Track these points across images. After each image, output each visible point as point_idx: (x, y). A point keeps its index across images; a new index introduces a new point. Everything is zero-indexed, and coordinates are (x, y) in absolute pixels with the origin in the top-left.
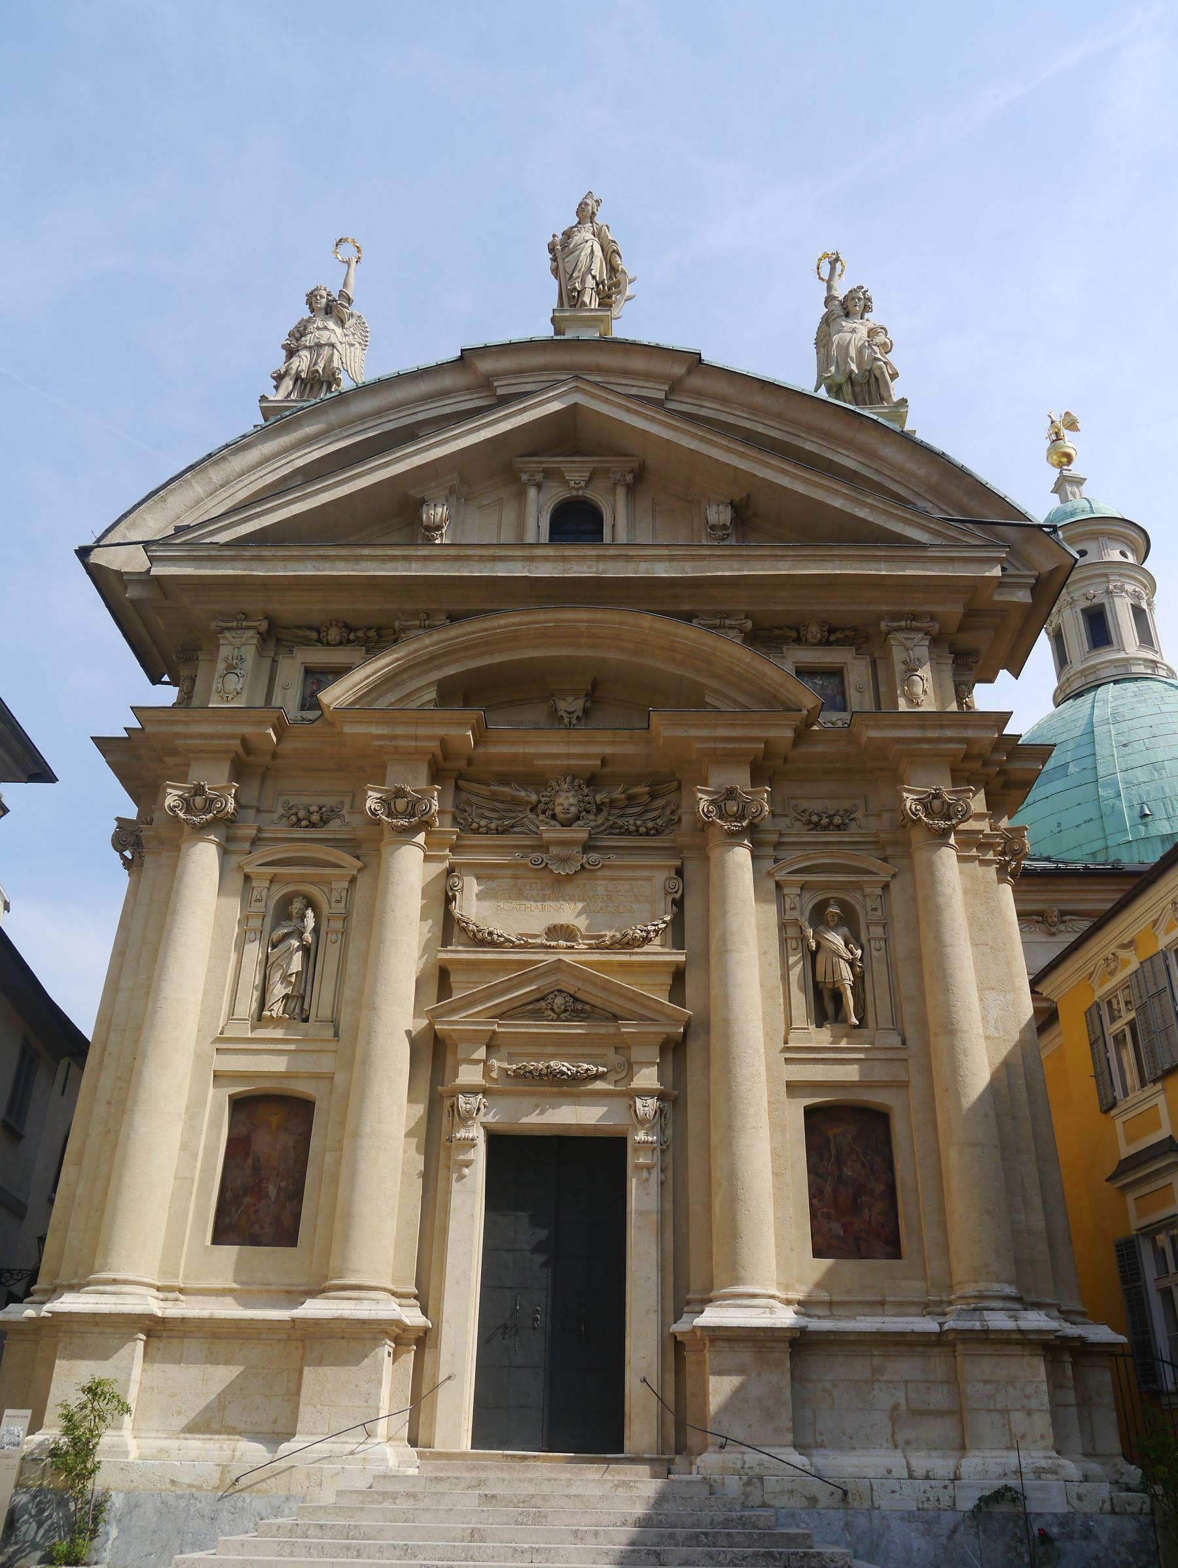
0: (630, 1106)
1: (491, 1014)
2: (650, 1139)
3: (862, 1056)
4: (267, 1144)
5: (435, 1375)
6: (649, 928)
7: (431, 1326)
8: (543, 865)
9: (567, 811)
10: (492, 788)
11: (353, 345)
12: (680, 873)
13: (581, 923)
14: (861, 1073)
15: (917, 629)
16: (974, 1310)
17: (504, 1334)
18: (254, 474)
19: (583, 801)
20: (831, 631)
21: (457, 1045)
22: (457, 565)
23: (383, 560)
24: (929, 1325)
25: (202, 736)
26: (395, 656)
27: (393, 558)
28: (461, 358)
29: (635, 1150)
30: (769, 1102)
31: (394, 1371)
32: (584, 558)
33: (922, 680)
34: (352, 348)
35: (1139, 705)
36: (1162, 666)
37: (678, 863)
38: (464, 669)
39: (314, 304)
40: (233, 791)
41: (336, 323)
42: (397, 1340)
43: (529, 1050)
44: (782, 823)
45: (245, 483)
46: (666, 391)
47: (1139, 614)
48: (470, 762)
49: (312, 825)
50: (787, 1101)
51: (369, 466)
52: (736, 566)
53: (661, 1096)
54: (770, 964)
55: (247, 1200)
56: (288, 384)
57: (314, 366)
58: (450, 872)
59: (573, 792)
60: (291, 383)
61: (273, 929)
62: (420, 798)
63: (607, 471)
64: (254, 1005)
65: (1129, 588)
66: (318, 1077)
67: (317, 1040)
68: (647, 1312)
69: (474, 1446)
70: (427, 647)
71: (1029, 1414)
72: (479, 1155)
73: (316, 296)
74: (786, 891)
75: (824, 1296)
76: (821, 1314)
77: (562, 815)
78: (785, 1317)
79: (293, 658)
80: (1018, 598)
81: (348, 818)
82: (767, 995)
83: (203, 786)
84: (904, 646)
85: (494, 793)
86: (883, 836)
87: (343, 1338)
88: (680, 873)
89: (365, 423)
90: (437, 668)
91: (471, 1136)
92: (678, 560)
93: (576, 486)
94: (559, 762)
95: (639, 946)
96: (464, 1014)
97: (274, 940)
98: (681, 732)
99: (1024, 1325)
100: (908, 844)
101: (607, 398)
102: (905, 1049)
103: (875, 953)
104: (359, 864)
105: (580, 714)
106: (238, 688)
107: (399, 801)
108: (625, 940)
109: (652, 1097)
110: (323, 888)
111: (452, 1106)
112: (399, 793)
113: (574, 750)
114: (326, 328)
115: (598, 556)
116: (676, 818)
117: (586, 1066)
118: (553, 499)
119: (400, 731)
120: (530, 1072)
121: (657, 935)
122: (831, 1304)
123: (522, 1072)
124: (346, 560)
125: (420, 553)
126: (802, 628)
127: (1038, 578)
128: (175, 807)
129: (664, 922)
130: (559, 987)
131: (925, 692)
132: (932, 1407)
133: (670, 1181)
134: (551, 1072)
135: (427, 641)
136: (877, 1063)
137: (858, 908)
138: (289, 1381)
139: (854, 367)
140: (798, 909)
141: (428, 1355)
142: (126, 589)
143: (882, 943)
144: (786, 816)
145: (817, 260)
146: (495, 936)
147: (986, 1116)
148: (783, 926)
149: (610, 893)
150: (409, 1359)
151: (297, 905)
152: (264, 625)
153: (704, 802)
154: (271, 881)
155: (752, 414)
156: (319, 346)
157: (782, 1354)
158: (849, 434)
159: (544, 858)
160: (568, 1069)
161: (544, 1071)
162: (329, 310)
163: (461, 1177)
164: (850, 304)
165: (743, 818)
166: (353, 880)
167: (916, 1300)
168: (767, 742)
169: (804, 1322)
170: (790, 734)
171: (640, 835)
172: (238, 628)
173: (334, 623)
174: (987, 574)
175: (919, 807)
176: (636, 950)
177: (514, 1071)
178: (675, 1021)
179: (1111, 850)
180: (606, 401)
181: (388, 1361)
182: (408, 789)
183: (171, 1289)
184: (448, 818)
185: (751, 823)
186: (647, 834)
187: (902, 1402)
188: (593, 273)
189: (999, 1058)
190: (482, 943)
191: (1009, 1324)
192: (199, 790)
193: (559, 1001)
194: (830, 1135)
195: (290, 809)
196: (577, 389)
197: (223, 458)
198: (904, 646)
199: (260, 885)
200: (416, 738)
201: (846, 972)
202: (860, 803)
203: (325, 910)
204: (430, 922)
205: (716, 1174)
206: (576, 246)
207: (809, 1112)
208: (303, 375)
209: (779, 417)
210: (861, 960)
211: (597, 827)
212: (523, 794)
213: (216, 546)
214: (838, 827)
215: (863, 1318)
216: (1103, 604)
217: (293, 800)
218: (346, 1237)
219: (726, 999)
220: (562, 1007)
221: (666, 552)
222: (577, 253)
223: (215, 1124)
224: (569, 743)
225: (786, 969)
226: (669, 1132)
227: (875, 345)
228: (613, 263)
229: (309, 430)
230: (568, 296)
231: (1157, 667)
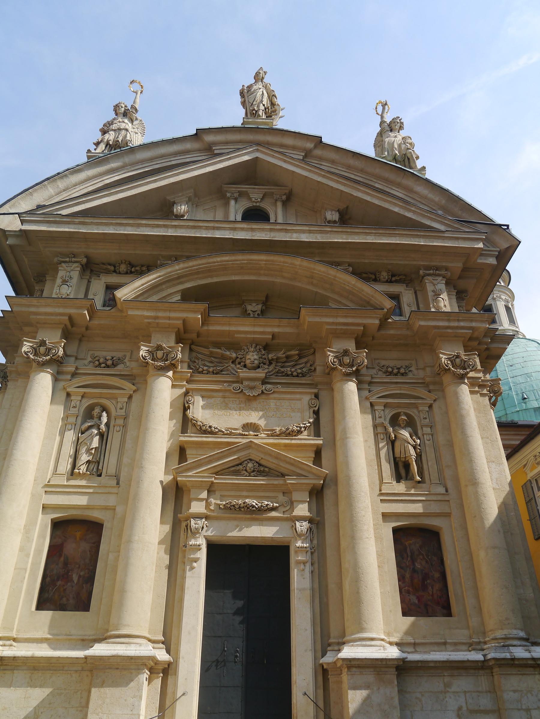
0: (293, 526)
1: (210, 472)
2: (305, 545)
3: (424, 498)
5: (174, 693)
6: (301, 425)
7: (172, 661)
8: (240, 391)
9: (253, 363)
10: (211, 349)
11: (137, 133)
12: (317, 396)
13: (262, 423)
14: (424, 507)
15: (439, 275)
16: (503, 646)
17: (217, 666)
18: (82, 185)
19: (261, 358)
20: (393, 276)
21: (190, 491)
22: (193, 231)
23: (153, 227)
24: (477, 656)
25: (46, 314)
26: (159, 274)
27: (158, 226)
28: (196, 134)
29: (296, 552)
30: (374, 525)
31: (149, 690)
32: (263, 230)
33: (443, 300)
34: (137, 135)
35: (515, 348)
36: (521, 334)
37: (316, 391)
38: (196, 284)
39: (118, 111)
40: (63, 344)
41: (129, 121)
42: (151, 670)
43: (232, 493)
44: (372, 372)
45: (77, 190)
46: (303, 155)
47: (508, 309)
48: (198, 335)
49: (108, 367)
50: (383, 524)
51: (146, 181)
52: (344, 237)
53: (311, 521)
54: (369, 447)
55: (59, 583)
56: (102, 147)
57: (117, 138)
58: (186, 394)
59: (256, 353)
60: (104, 146)
61: (82, 424)
62: (170, 351)
63: (272, 193)
64: (69, 466)
65: (503, 297)
66: (106, 508)
67: (106, 487)
68: (306, 651)
70: (177, 270)
72: (203, 555)
73: (119, 106)
74: (376, 408)
75: (410, 640)
76: (409, 651)
77: (250, 365)
78: (393, 653)
79: (100, 279)
80: (490, 262)
81: (128, 364)
82: (369, 465)
83: (45, 341)
84: (432, 283)
85: (211, 352)
86: (428, 379)
87: (117, 669)
88: (317, 396)
89: (143, 164)
90: (182, 283)
91: (198, 543)
92: (313, 233)
94: (249, 336)
95: (295, 436)
96: (195, 472)
97: (83, 430)
98: (317, 319)
100: (441, 383)
101: (274, 155)
102: (448, 494)
103: (427, 442)
104: (134, 388)
105: (259, 312)
106: (68, 292)
107: (159, 352)
108: (288, 431)
109: (305, 521)
110: (112, 401)
111: (187, 526)
112: (159, 348)
113: (257, 329)
114: (123, 122)
115: (271, 229)
116: (313, 368)
117: (266, 503)
118: (244, 206)
119: (160, 314)
120: (234, 506)
121: (305, 430)
122: (415, 645)
123: (229, 506)
124: (132, 226)
125: (173, 224)
126: (377, 273)
127: (499, 252)
128: (28, 352)
129: (309, 423)
130: (250, 457)
131: (445, 306)
132: (482, 708)
133: (317, 570)
134: (246, 506)
135: (177, 267)
136: (432, 502)
137: (416, 417)
138: (81, 698)
139: (397, 152)
140: (383, 418)
142: (7, 240)
143: (431, 436)
144: (373, 368)
145: (376, 104)
146: (213, 428)
147: (499, 531)
148: (375, 427)
149: (278, 407)
150: (158, 682)
151: (97, 410)
152: (85, 260)
153: (331, 357)
154: (82, 397)
155: (347, 169)
156: (120, 129)
157: (392, 675)
158: (399, 180)
159: (241, 387)
160: (256, 504)
161: (242, 505)
162: (125, 114)
163: (192, 568)
164: (393, 125)
165: (352, 366)
166: (130, 397)
167: (465, 641)
168: (365, 326)
169: (404, 655)
170: (377, 322)
171: (294, 377)
172: (69, 262)
173: (124, 262)
174: (475, 246)
175: (449, 362)
176: (294, 437)
177: (224, 505)
178: (318, 477)
179: (509, 416)
180: (273, 156)
181: (146, 683)
182: (164, 345)
183: (8, 639)
184: (186, 365)
185: (357, 370)
186: (297, 376)
187: (464, 705)
188: (263, 103)
189: (501, 500)
190: (205, 432)
191: (527, 655)
192: (43, 343)
193: (250, 465)
194: (407, 544)
195: (95, 358)
196: (257, 150)
197: (66, 176)
198: (432, 283)
199: (75, 399)
200: (169, 318)
201: (412, 452)
202: (413, 362)
203: (113, 413)
204: (174, 421)
205: (346, 565)
206: (255, 90)
207: (395, 531)
208: (111, 143)
209: (362, 171)
210: (419, 445)
211: (269, 372)
212: (228, 353)
213: (60, 216)
214: (402, 374)
215: (434, 653)
216: (491, 305)
217: (97, 353)
218: (121, 604)
219: (347, 464)
220: (252, 469)
221: (307, 228)
222: (256, 93)
223: (42, 536)
224: (254, 325)
225: (378, 450)
226: (315, 542)
227: (407, 143)
228: (273, 101)
229: (113, 165)
230: (251, 114)
231: (518, 334)
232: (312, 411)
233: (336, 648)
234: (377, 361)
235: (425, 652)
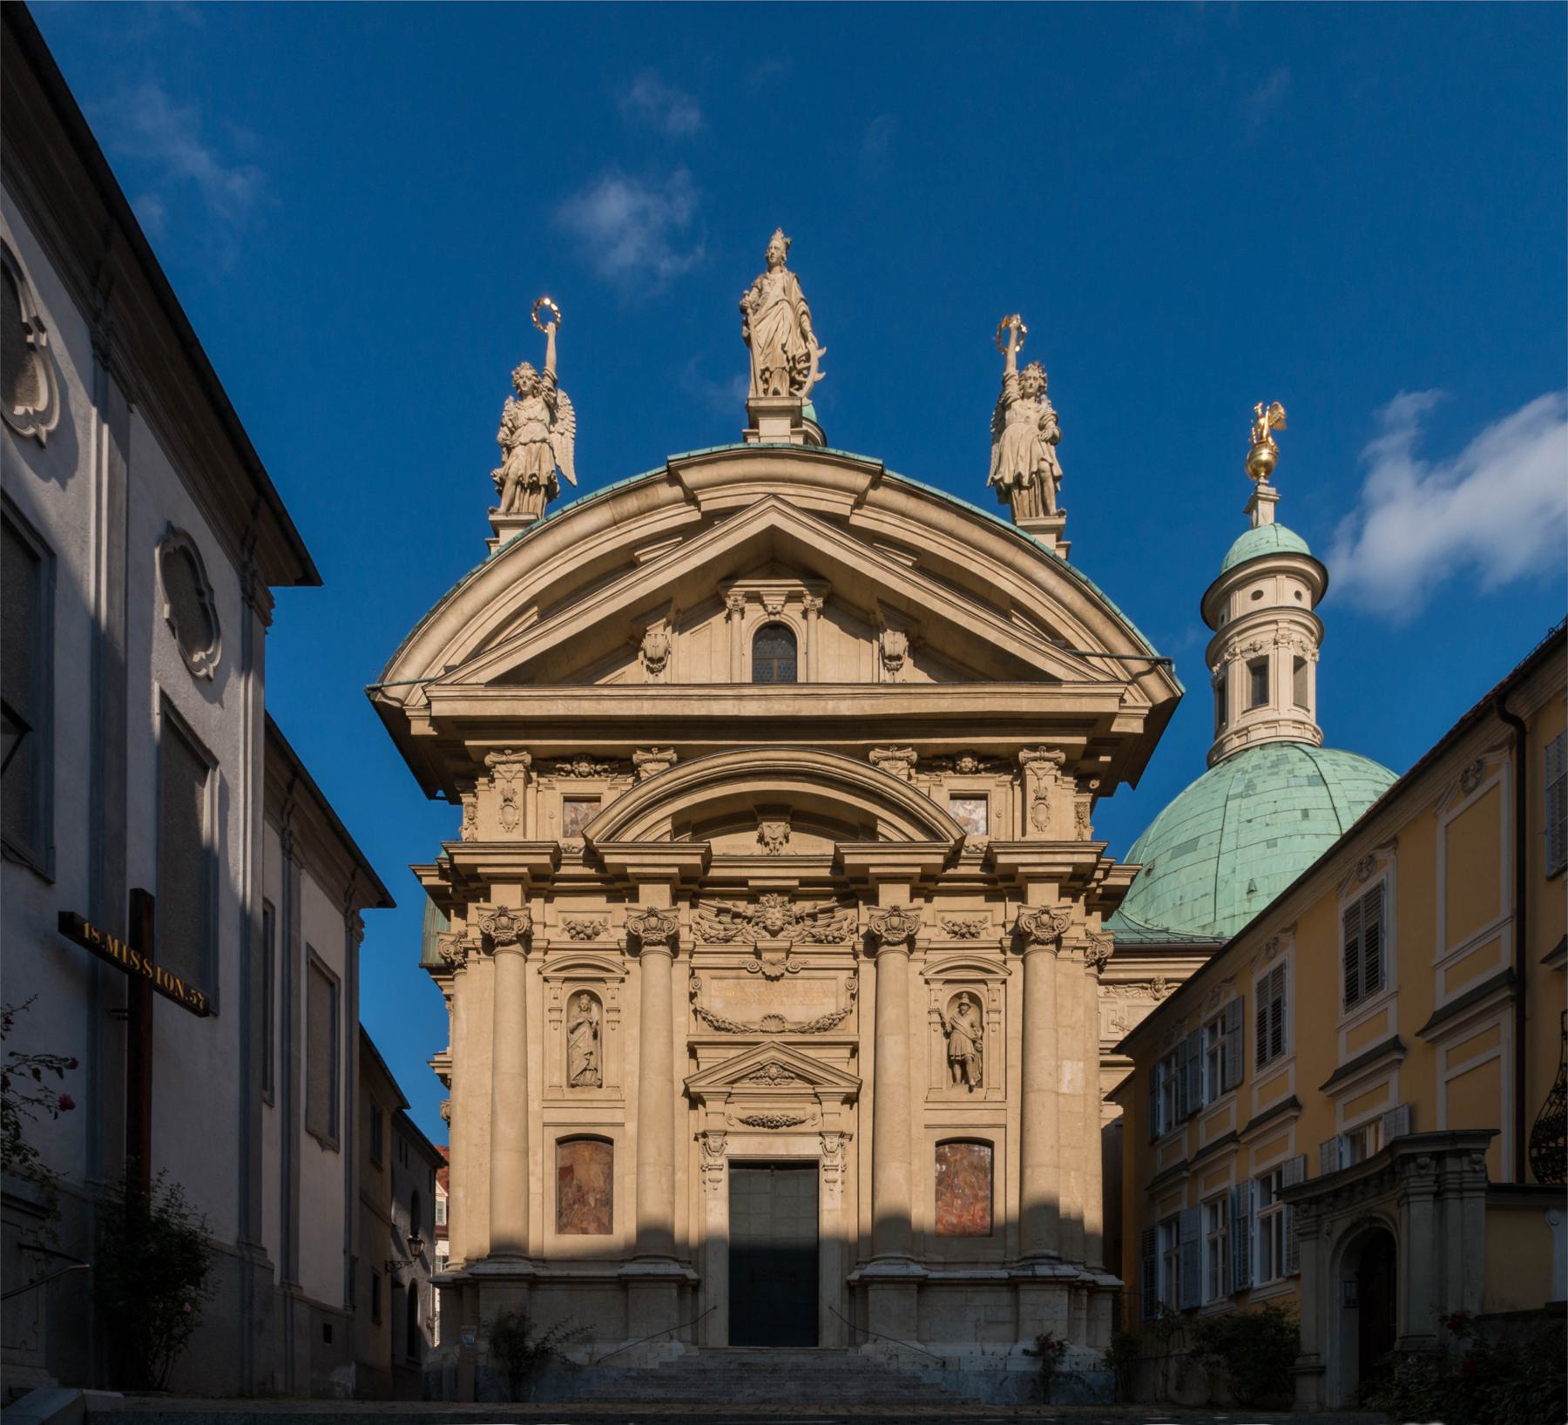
4: (588, 1173)
6: (835, 1017)
12: (856, 971)
24: (1004, 1274)
69: (731, 1343)
71: (1055, 1322)
72: (724, 1175)
93: (774, 611)
99: (1057, 1273)
111: (705, 1144)
137: (982, 999)
141: (701, 1296)
144: (935, 926)
171: (829, 942)
186: (834, 941)
190: (718, 1029)
193: (774, 1071)
201: (969, 1049)
208: (526, 481)
214: (973, 935)
232: (849, 992)
233: (864, 1266)
234: (942, 914)
235: (955, 1271)
